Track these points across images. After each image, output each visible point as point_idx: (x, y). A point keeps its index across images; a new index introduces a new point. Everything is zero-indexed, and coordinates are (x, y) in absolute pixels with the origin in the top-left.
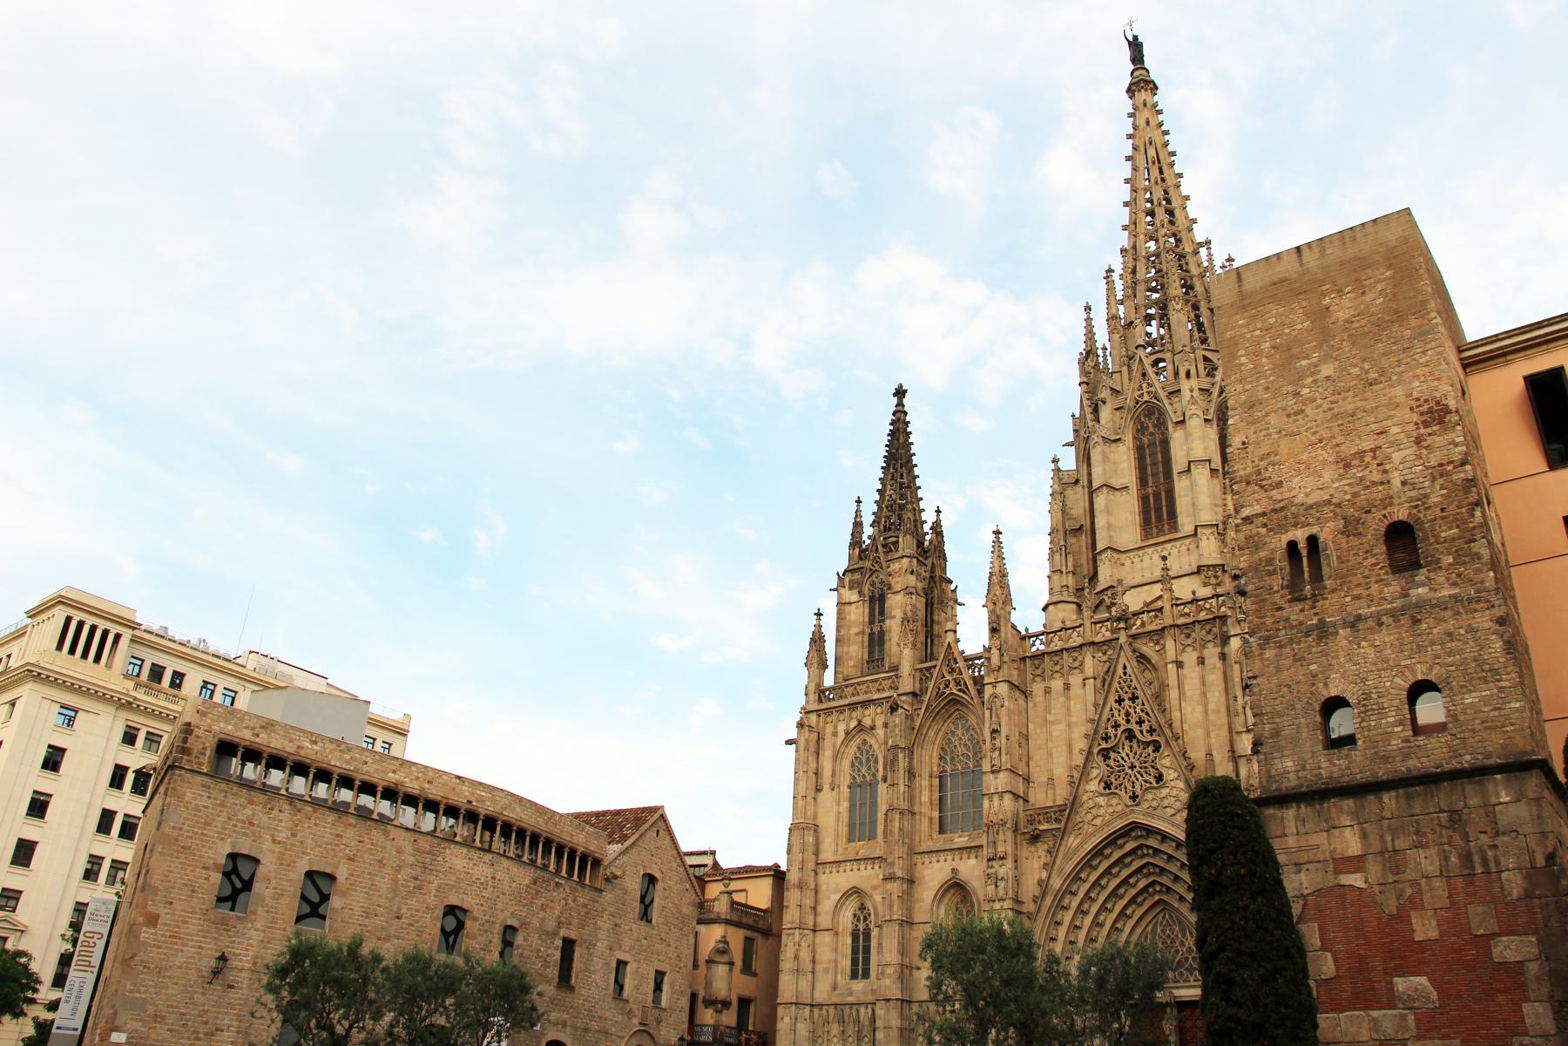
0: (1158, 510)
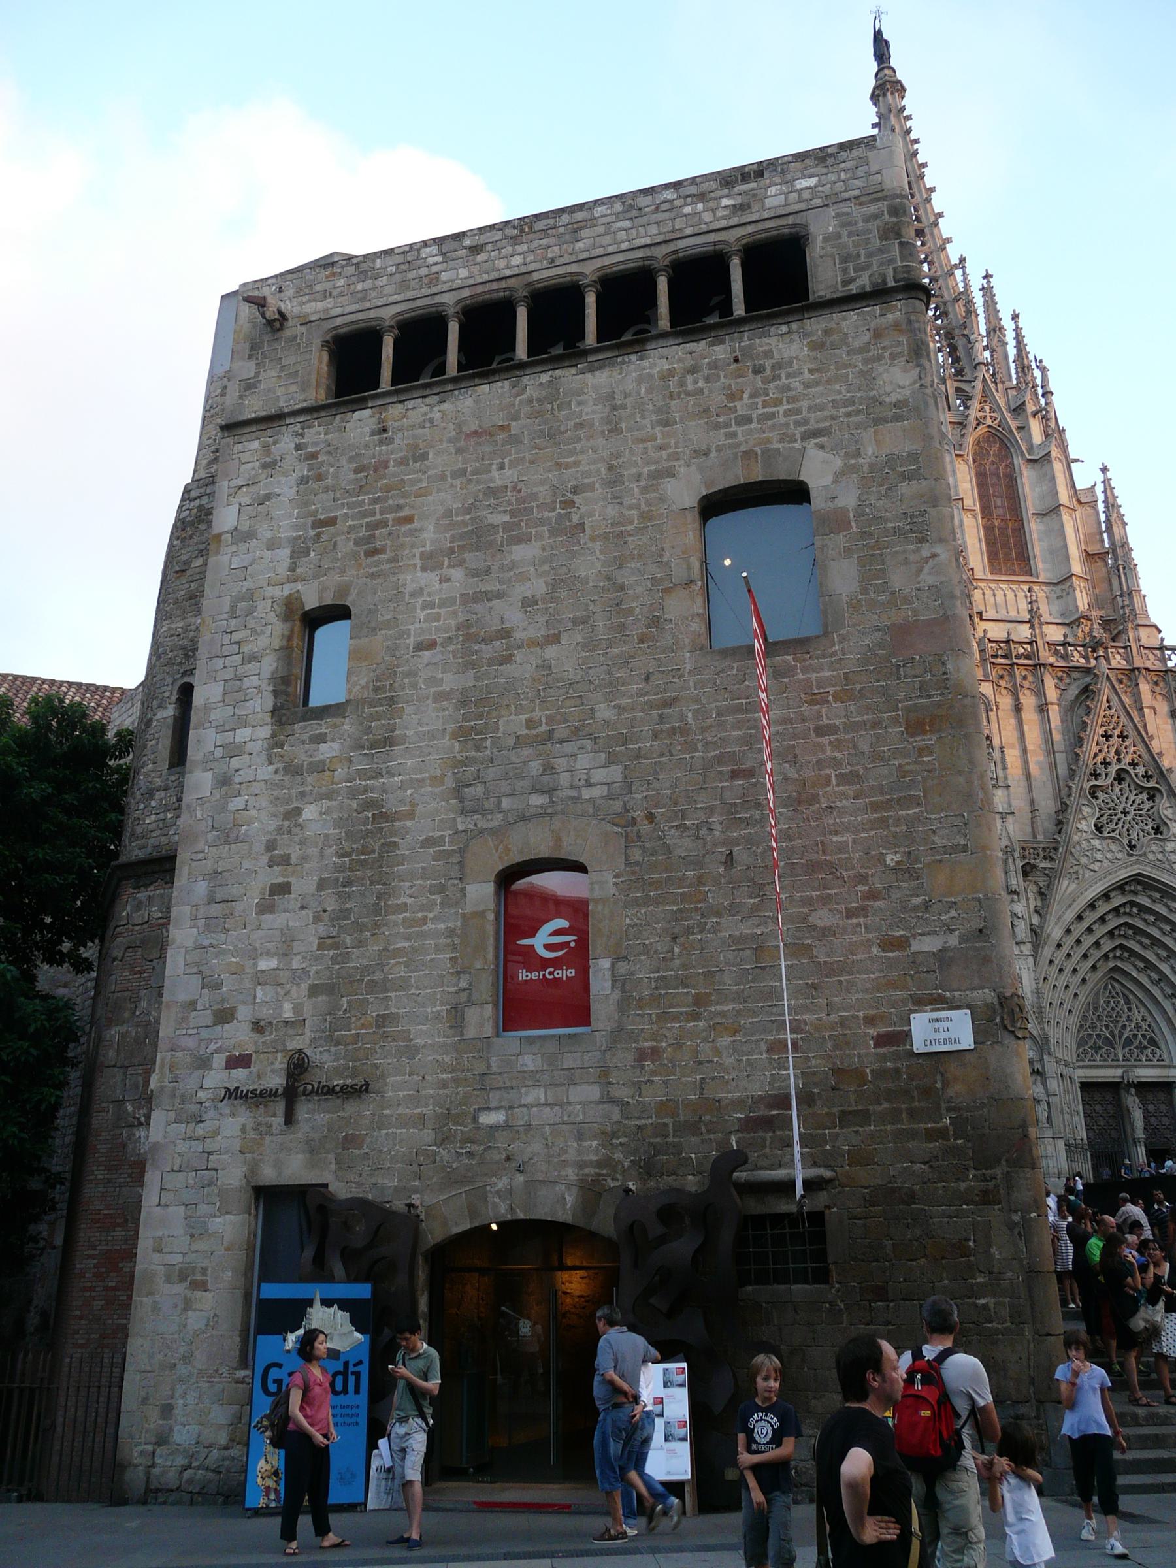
0: (1006, 545)
